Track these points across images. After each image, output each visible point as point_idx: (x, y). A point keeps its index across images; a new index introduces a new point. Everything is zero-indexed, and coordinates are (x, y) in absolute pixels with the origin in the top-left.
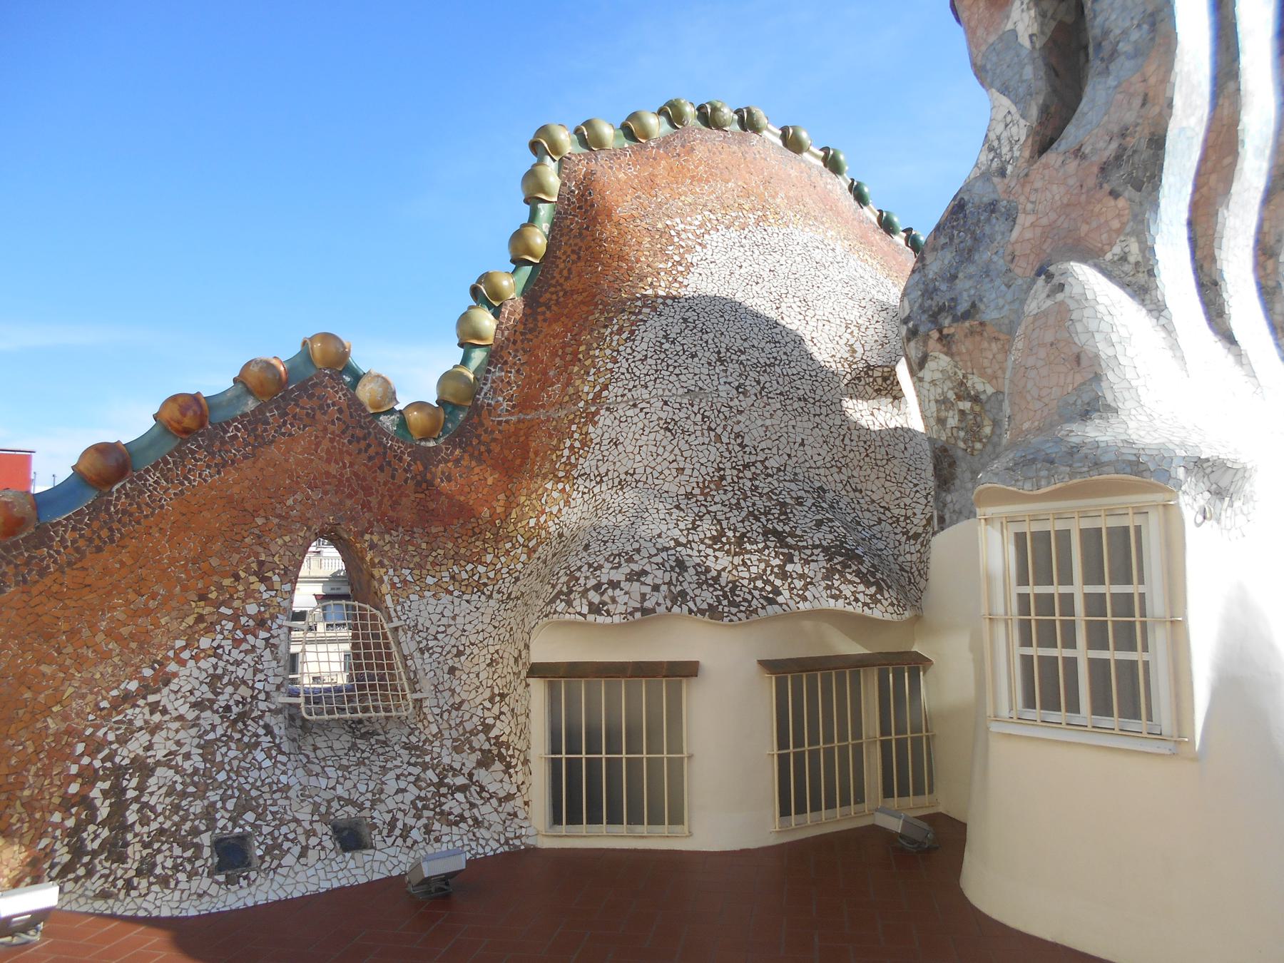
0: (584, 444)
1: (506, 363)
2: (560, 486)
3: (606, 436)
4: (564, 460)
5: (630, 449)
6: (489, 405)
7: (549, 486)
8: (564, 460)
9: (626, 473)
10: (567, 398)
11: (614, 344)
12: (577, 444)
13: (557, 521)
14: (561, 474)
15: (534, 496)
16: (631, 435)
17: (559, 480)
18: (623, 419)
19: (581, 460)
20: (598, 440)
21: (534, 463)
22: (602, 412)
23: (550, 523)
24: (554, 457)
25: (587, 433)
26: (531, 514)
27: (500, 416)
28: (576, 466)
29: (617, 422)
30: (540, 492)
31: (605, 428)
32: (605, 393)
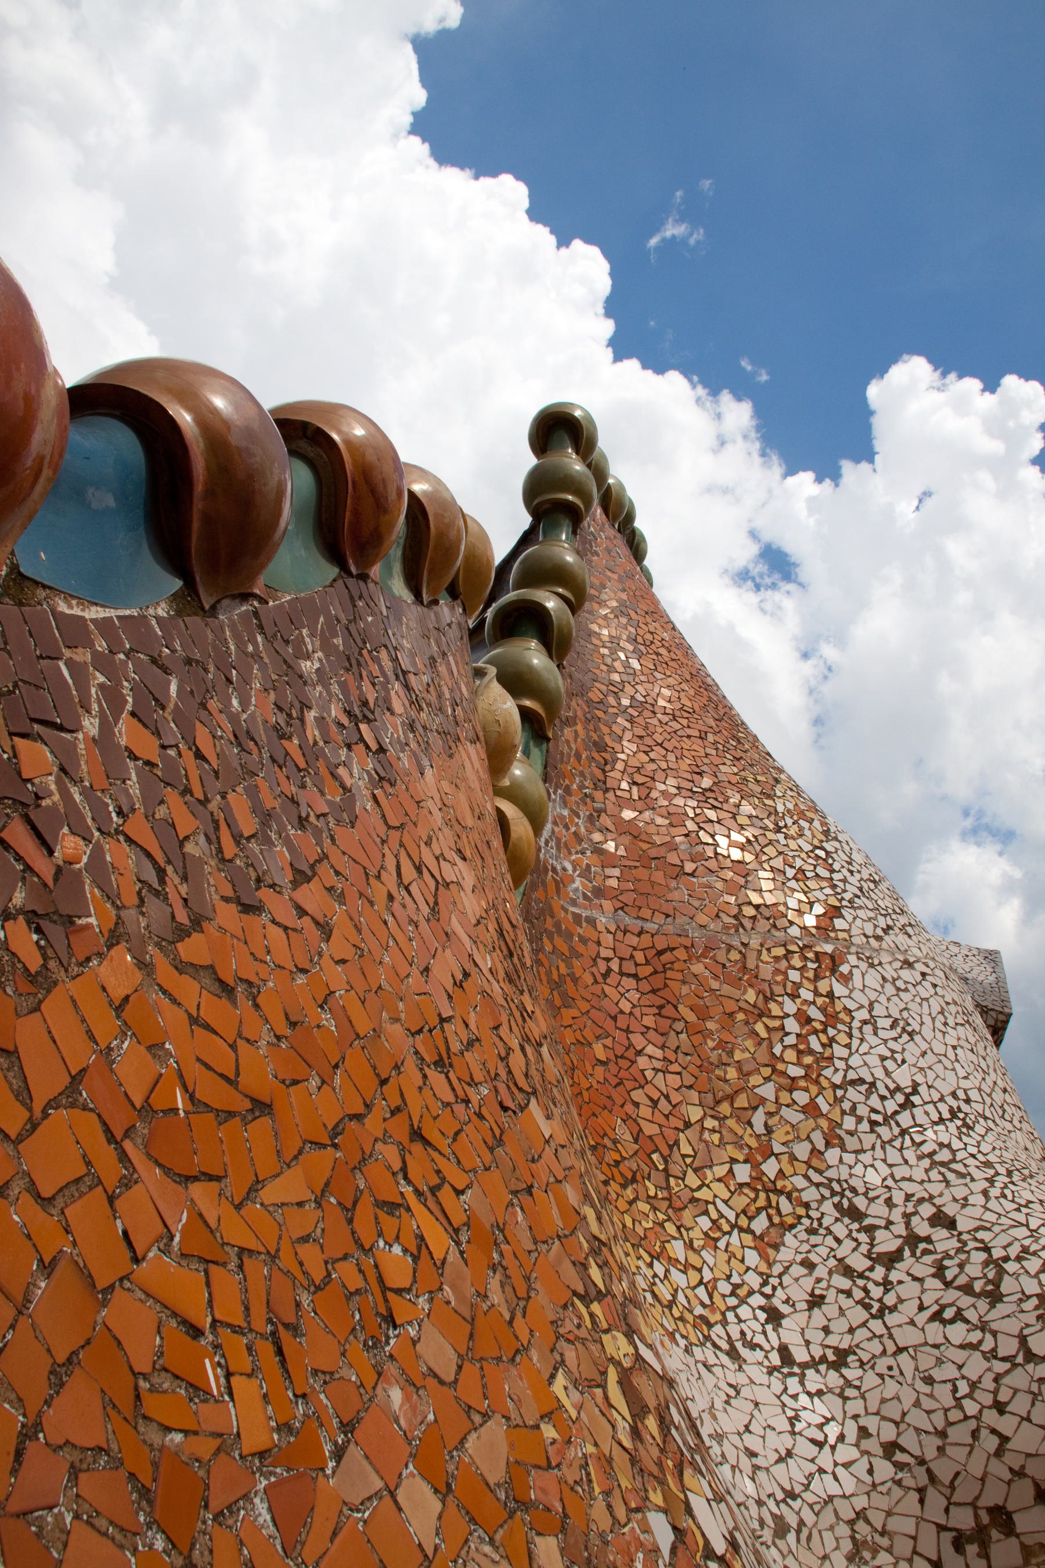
0: (831, 1019)
1: (567, 790)
2: (801, 1098)
3: (879, 1010)
4: (791, 1040)
5: (939, 1048)
6: (554, 870)
7: (768, 1091)
8: (791, 1040)
9: (954, 1095)
10: (749, 911)
11: (807, 833)
12: (814, 1013)
13: (816, 1178)
14: (795, 1071)
15: (725, 1108)
16: (927, 1020)
17: (792, 1085)
18: (900, 984)
19: (839, 1051)
20: (864, 1014)
21: (697, 1032)
22: (852, 959)
23: (800, 1182)
24: (759, 1028)
25: (830, 995)
26: (731, 1151)
27: (574, 903)
28: (831, 1058)
29: (890, 989)
30: (742, 1101)
31: (873, 996)
32: (839, 923)
